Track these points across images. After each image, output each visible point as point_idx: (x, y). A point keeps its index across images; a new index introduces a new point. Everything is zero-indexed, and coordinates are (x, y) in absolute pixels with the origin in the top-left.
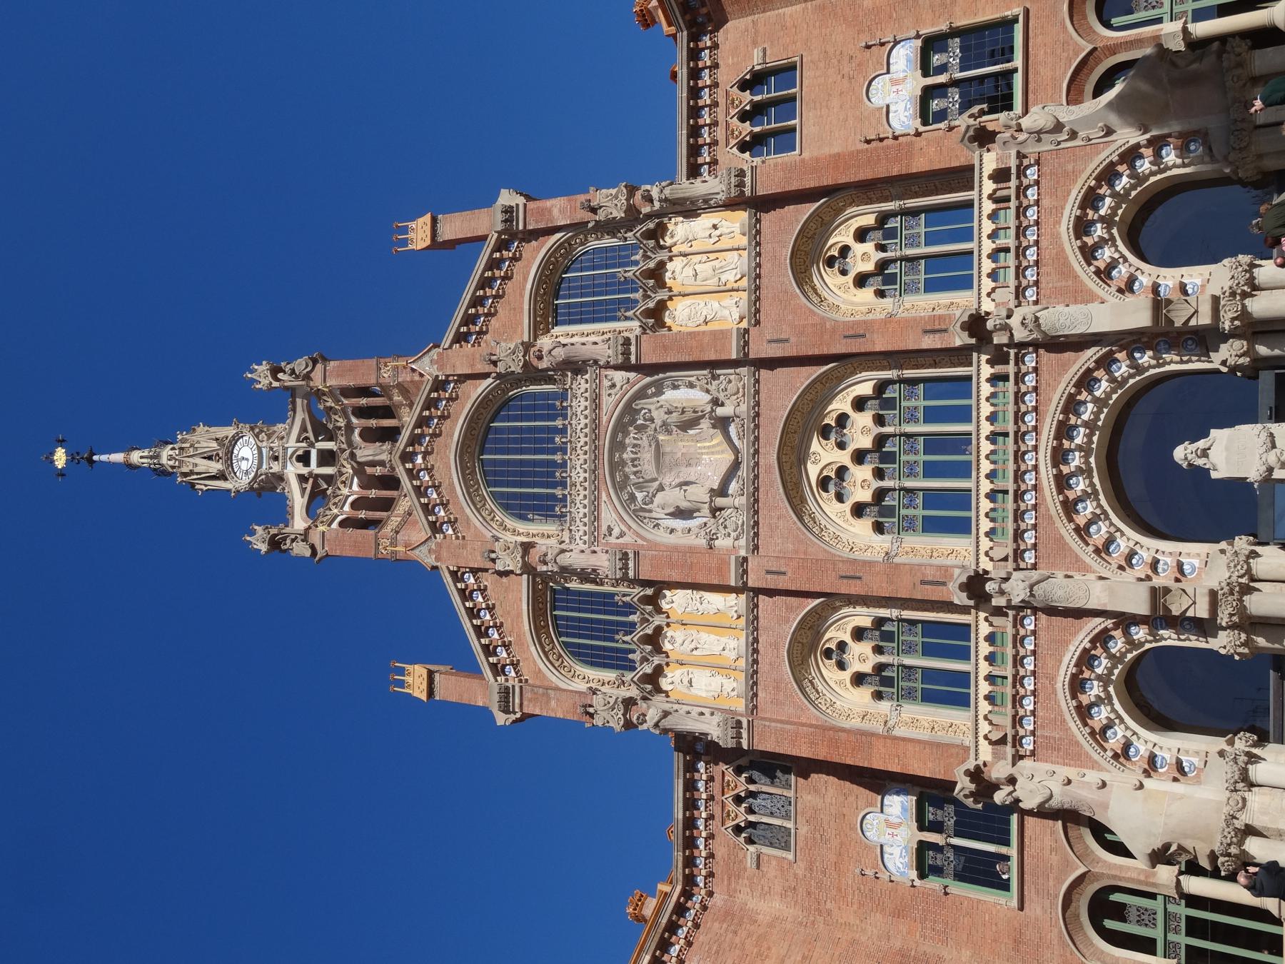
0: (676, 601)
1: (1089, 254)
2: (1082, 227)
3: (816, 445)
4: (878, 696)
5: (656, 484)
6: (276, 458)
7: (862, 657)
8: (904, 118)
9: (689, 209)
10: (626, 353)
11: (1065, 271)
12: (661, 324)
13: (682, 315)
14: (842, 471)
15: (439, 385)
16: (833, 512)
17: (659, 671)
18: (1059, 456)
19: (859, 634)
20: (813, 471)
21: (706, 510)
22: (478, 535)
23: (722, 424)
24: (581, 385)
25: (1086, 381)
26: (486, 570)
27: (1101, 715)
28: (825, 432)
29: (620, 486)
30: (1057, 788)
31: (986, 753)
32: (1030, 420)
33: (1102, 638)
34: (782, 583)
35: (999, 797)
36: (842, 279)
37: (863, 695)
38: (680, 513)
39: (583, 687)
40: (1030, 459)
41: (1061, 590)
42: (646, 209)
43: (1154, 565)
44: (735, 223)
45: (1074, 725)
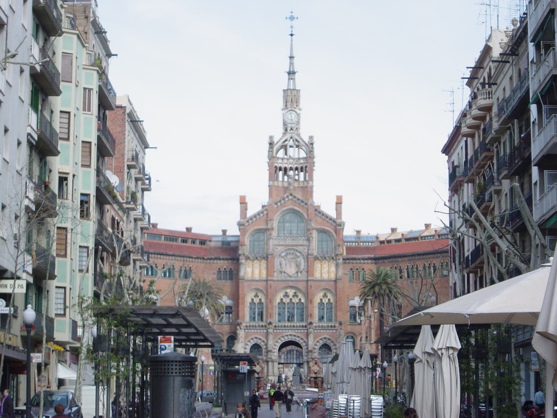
0: (264, 262)
1: (321, 339)
2: (325, 338)
3: (293, 291)
4: (250, 303)
5: (286, 258)
6: (291, 129)
7: (256, 300)
8: (352, 303)
9: (337, 265)
10: (310, 255)
11: (319, 336)
12: (315, 260)
13: (318, 265)
14: (288, 296)
15: (306, 204)
16: (280, 295)
17: (250, 260)
18: (291, 335)
19: (260, 300)
20: (288, 291)
21: (281, 270)
22: (275, 214)
23: (297, 272)
24: (305, 243)
25: (302, 339)
26: (267, 217)
27: (252, 341)
28: (295, 293)
29: (286, 250)
30: (241, 335)
31: (244, 324)
32: (296, 331)
33: (263, 341)
34: (269, 288)
35: (238, 327)
36: (322, 296)
37: (249, 300)
38: (281, 264)
39: (246, 243)
40: (290, 331)
41: (271, 337)
42: (337, 258)
43: (275, 349)
44: (333, 276)
45: (250, 338)
